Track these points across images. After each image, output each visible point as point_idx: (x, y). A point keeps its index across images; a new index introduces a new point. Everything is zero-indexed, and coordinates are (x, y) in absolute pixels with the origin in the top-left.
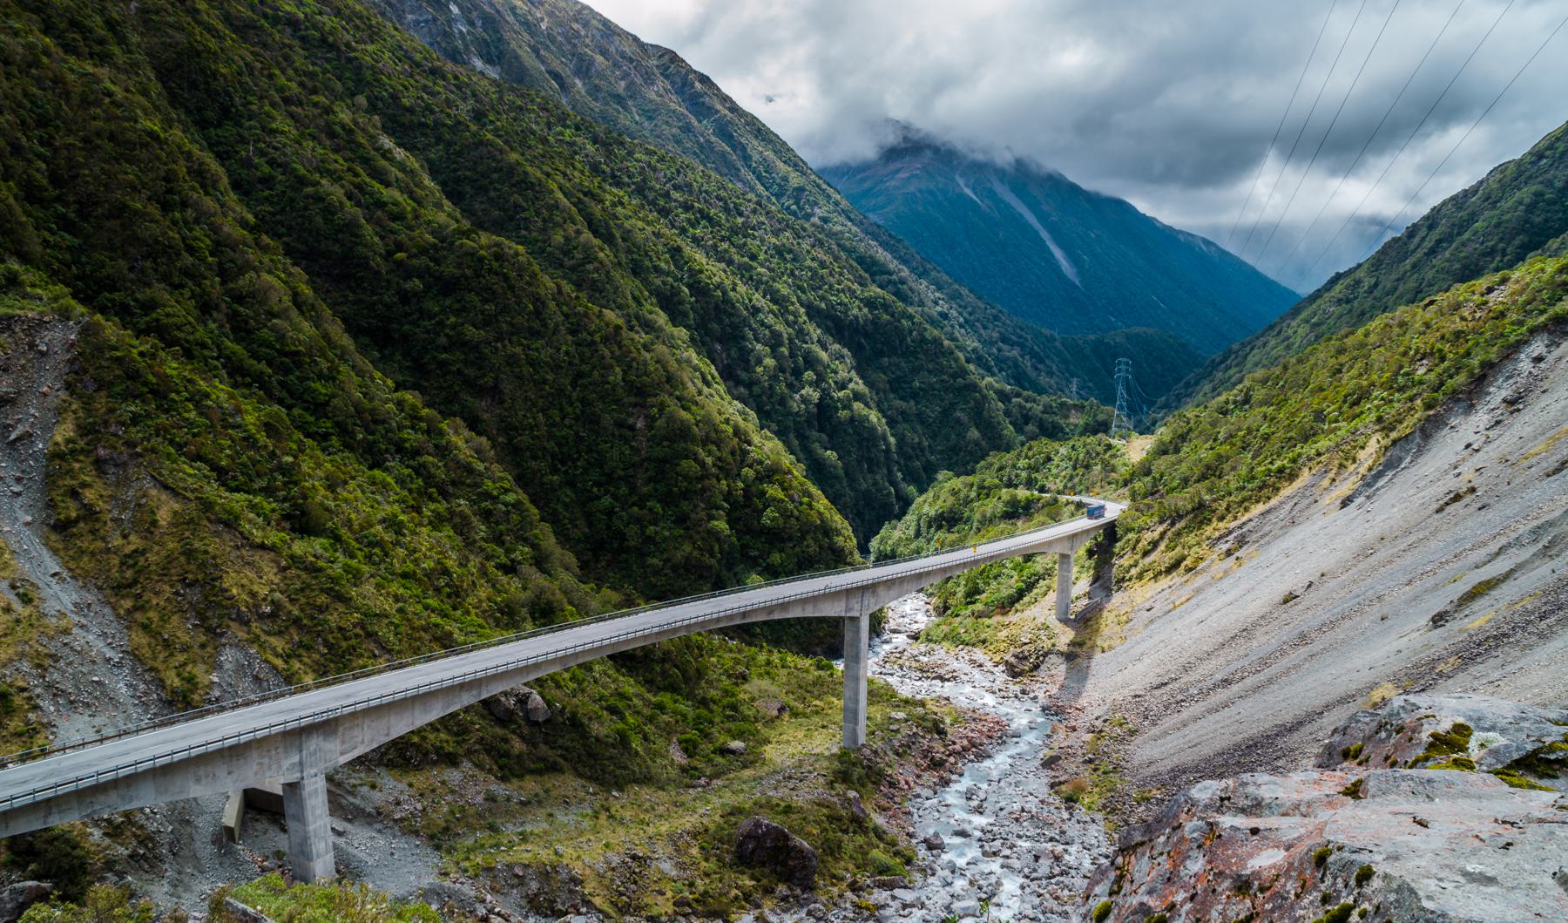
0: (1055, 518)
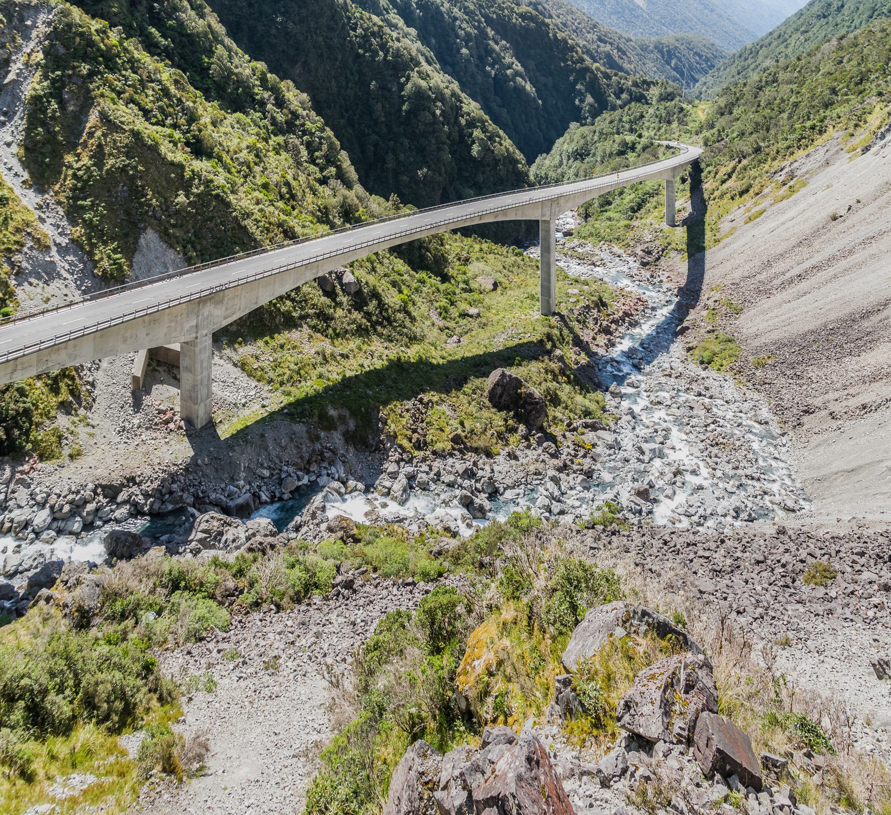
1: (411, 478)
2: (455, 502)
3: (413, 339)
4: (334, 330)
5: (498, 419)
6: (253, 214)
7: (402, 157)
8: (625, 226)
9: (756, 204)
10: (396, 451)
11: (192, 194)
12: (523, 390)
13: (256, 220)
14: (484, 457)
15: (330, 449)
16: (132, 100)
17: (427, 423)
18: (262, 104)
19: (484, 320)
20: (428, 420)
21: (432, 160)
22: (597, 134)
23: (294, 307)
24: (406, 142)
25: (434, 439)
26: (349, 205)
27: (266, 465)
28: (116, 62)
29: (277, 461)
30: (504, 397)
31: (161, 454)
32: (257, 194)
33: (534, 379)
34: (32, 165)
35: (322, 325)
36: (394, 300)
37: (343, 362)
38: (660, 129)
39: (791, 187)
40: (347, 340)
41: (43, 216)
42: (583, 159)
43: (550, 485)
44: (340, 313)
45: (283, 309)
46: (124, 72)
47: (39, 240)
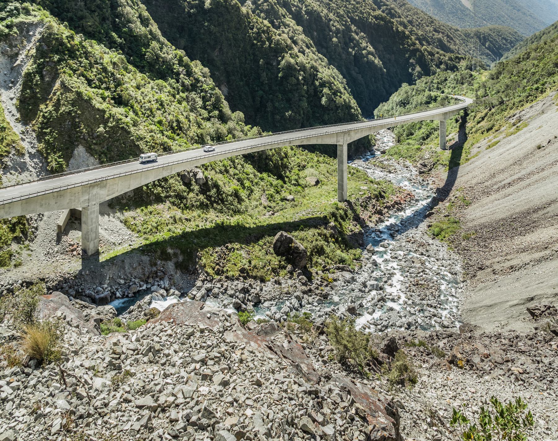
1: (209, 290)
2: (231, 306)
3: (237, 212)
4: (185, 205)
5: (275, 260)
6: (145, 138)
7: (277, 104)
8: (417, 149)
9: (495, 137)
10: (204, 274)
11: (108, 126)
12: (293, 245)
13: (146, 141)
14: (259, 282)
15: (162, 271)
16: (83, 76)
17: (227, 260)
18: (178, 74)
19: (296, 203)
20: (228, 258)
21: (295, 106)
22: (415, 91)
23: (163, 191)
24: (280, 96)
25: (229, 269)
26: (221, 133)
27: (122, 277)
28: (76, 54)
29: (129, 276)
30: (282, 248)
31: (63, 268)
32: (153, 127)
33: (308, 239)
34: (22, 110)
35: (177, 201)
36: (228, 189)
37: (186, 223)
38: (455, 88)
39: (517, 127)
40: (192, 211)
41: (24, 137)
42: (405, 106)
44: (191, 195)
45: (155, 191)
46: (80, 59)
47: (18, 150)
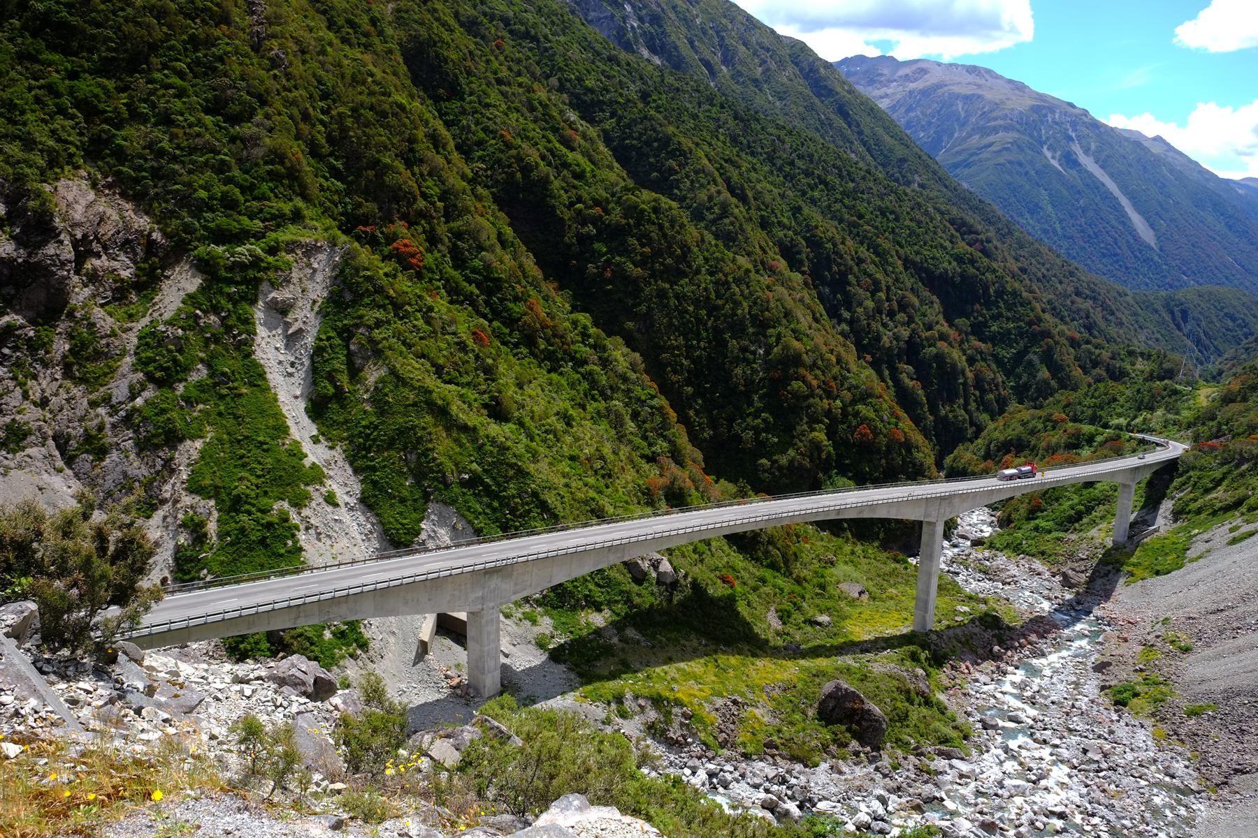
0: (1119, 453)
18: (580, 363)
43: (877, 806)
